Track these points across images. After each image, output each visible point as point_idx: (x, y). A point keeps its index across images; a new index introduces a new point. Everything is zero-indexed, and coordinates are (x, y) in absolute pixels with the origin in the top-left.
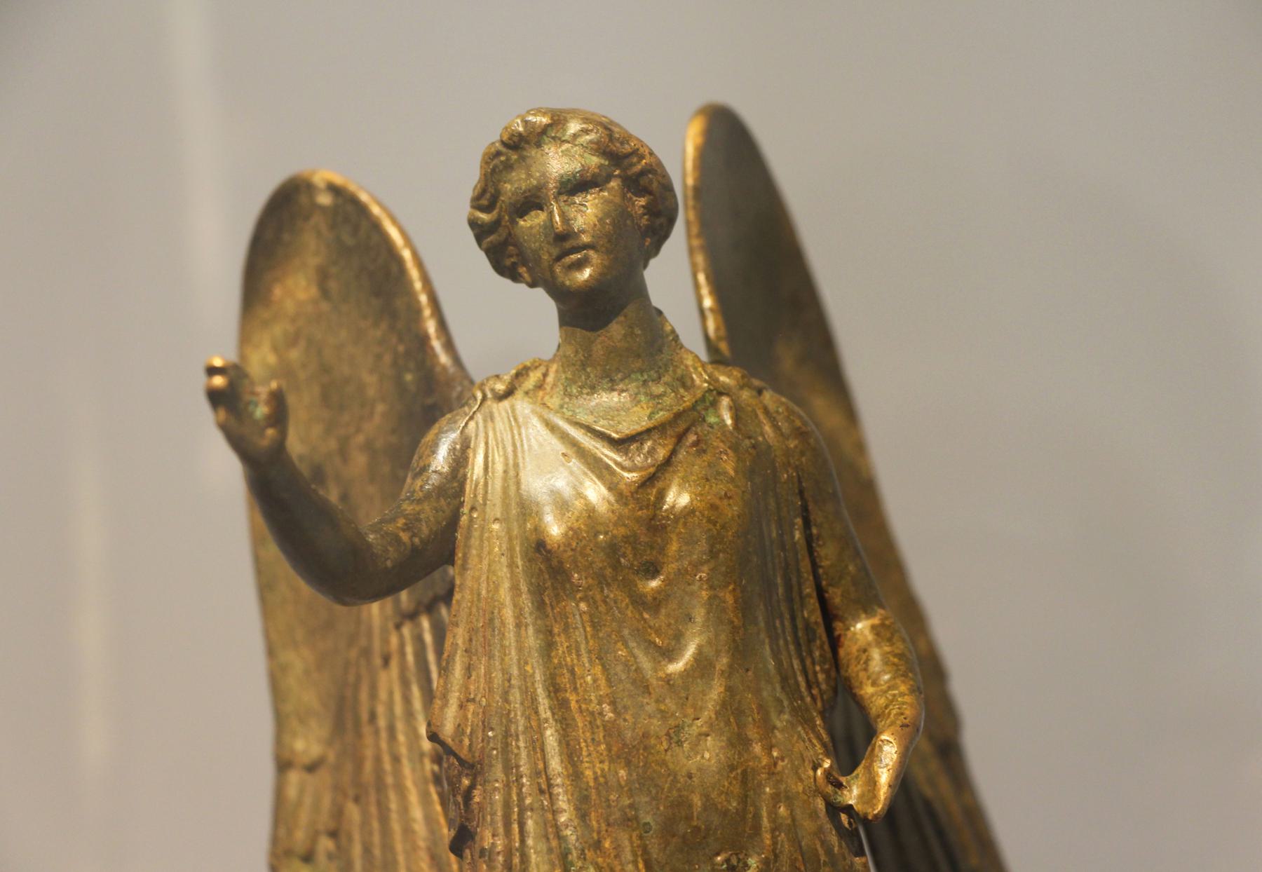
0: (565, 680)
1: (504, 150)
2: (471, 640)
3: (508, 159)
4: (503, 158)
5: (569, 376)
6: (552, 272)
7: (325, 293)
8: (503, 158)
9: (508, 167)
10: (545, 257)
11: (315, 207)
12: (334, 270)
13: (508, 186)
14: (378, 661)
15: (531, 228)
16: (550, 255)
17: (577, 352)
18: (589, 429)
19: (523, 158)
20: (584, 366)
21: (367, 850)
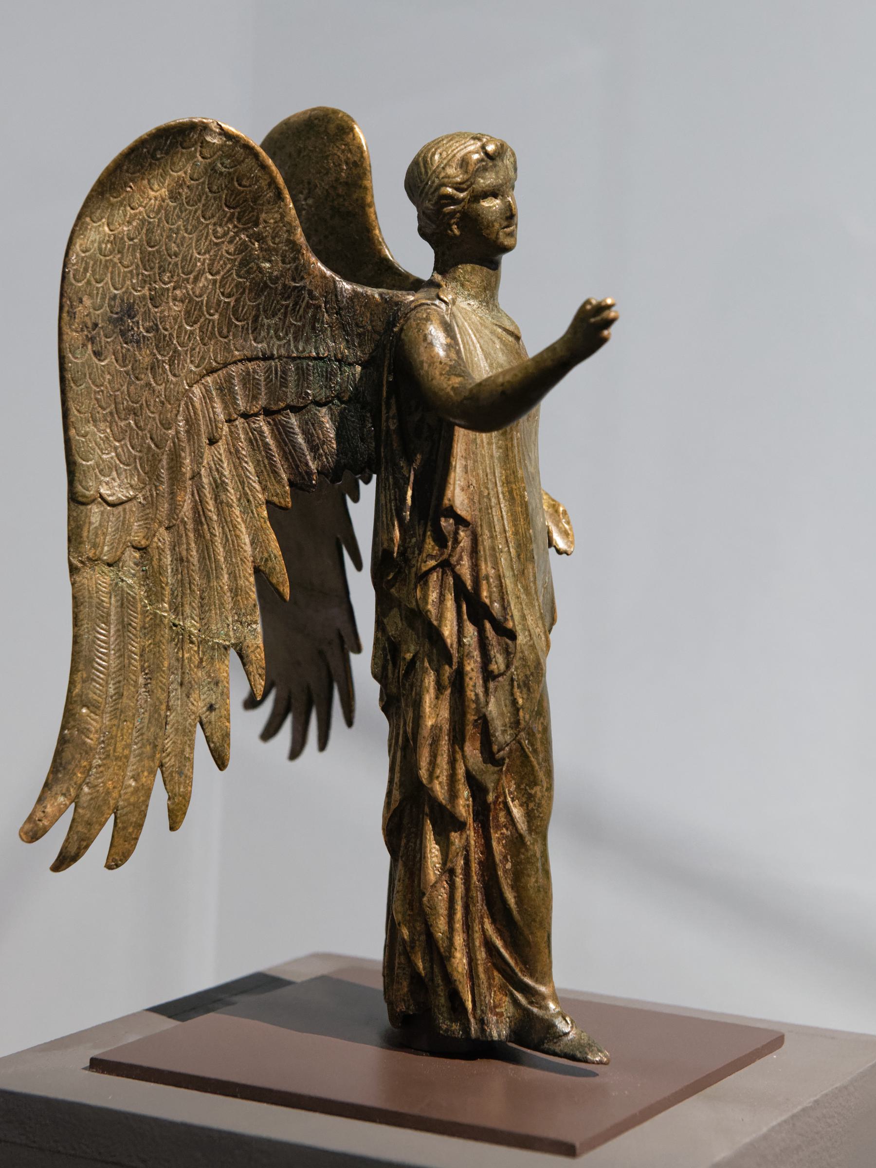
0: (512, 479)
1: (486, 159)
2: (507, 456)
3: (487, 164)
4: (484, 163)
5: (472, 293)
6: (498, 234)
7: (174, 196)
8: (484, 163)
9: (485, 169)
10: (497, 225)
11: (204, 143)
12: (189, 182)
13: (482, 181)
14: (205, 440)
15: (490, 207)
16: (501, 225)
17: (483, 281)
18: (505, 330)
19: (495, 166)
20: (485, 289)
21: (180, 560)
